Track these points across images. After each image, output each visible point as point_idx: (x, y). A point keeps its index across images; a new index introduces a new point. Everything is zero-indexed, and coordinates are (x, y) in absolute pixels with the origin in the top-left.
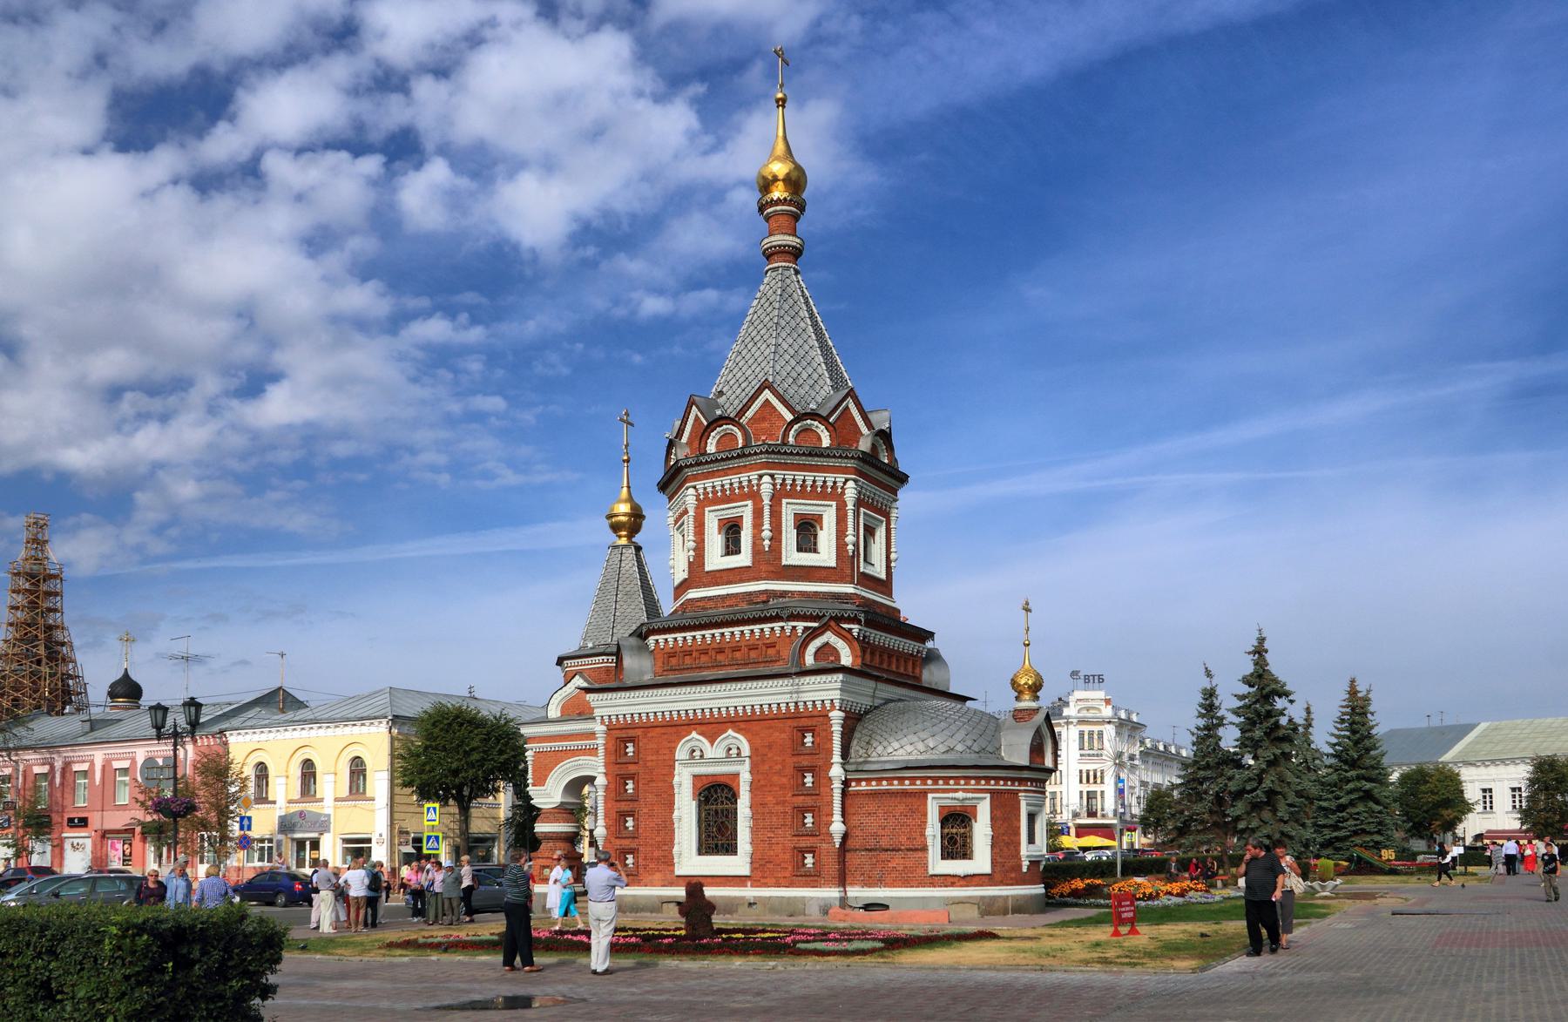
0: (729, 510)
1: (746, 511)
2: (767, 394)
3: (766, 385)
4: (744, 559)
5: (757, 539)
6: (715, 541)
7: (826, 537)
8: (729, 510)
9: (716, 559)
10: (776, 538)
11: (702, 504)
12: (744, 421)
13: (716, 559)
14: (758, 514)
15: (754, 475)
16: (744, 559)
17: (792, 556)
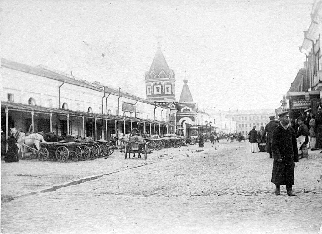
0: (158, 86)
1: (160, 86)
2: (162, 71)
3: (163, 69)
4: (160, 93)
5: (162, 91)
6: (155, 90)
7: (170, 90)
8: (158, 86)
9: (156, 93)
10: (165, 91)
11: (154, 85)
12: (160, 74)
13: (156, 93)
14: (162, 87)
15: (161, 82)
16: (160, 93)
17: (166, 93)
